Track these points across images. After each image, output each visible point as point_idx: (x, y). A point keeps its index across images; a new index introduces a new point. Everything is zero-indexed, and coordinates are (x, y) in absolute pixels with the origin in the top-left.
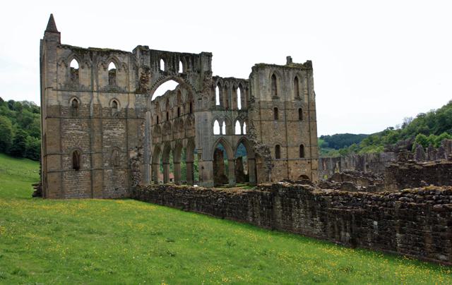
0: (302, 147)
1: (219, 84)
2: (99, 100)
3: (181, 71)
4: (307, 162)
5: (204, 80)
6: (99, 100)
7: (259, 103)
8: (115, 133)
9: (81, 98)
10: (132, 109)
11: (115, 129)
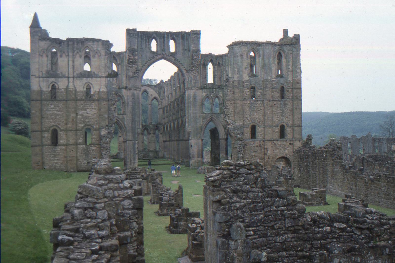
1: (211, 61)
3: (172, 49)
4: (288, 144)
5: (192, 59)
7: (233, 82)
8: (87, 113)
9: (59, 84)
10: (103, 92)
11: (88, 110)
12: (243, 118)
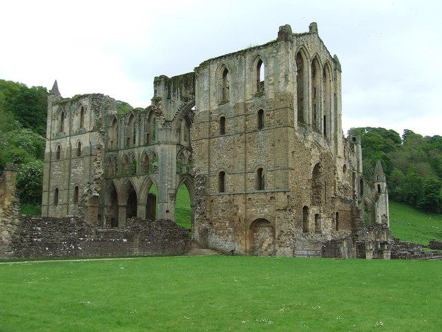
2: (70, 144)
6: (70, 144)
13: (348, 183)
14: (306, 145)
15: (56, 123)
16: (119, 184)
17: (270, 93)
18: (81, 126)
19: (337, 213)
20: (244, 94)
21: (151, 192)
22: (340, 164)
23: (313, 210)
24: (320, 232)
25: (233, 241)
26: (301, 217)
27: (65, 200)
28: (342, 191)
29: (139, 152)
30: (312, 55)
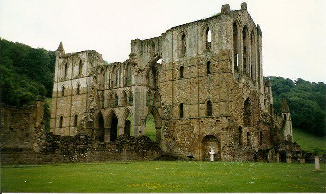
0: (209, 103)
12: (173, 98)
13: (267, 111)
14: (240, 85)
15: (62, 71)
16: (106, 114)
17: (215, 50)
18: (80, 72)
19: (261, 133)
20: (195, 51)
21: (128, 118)
22: (262, 98)
23: (245, 130)
24: (251, 145)
25: (189, 151)
26: (237, 134)
27: (68, 125)
28: (264, 117)
29: (120, 92)
30: (243, 24)
